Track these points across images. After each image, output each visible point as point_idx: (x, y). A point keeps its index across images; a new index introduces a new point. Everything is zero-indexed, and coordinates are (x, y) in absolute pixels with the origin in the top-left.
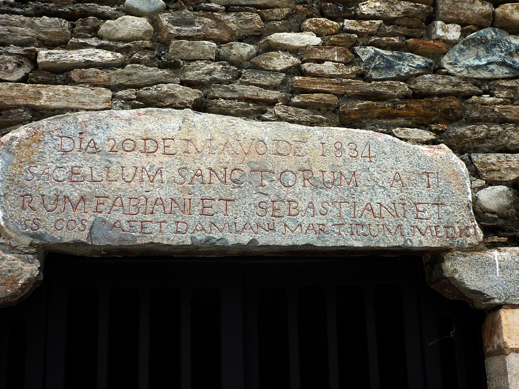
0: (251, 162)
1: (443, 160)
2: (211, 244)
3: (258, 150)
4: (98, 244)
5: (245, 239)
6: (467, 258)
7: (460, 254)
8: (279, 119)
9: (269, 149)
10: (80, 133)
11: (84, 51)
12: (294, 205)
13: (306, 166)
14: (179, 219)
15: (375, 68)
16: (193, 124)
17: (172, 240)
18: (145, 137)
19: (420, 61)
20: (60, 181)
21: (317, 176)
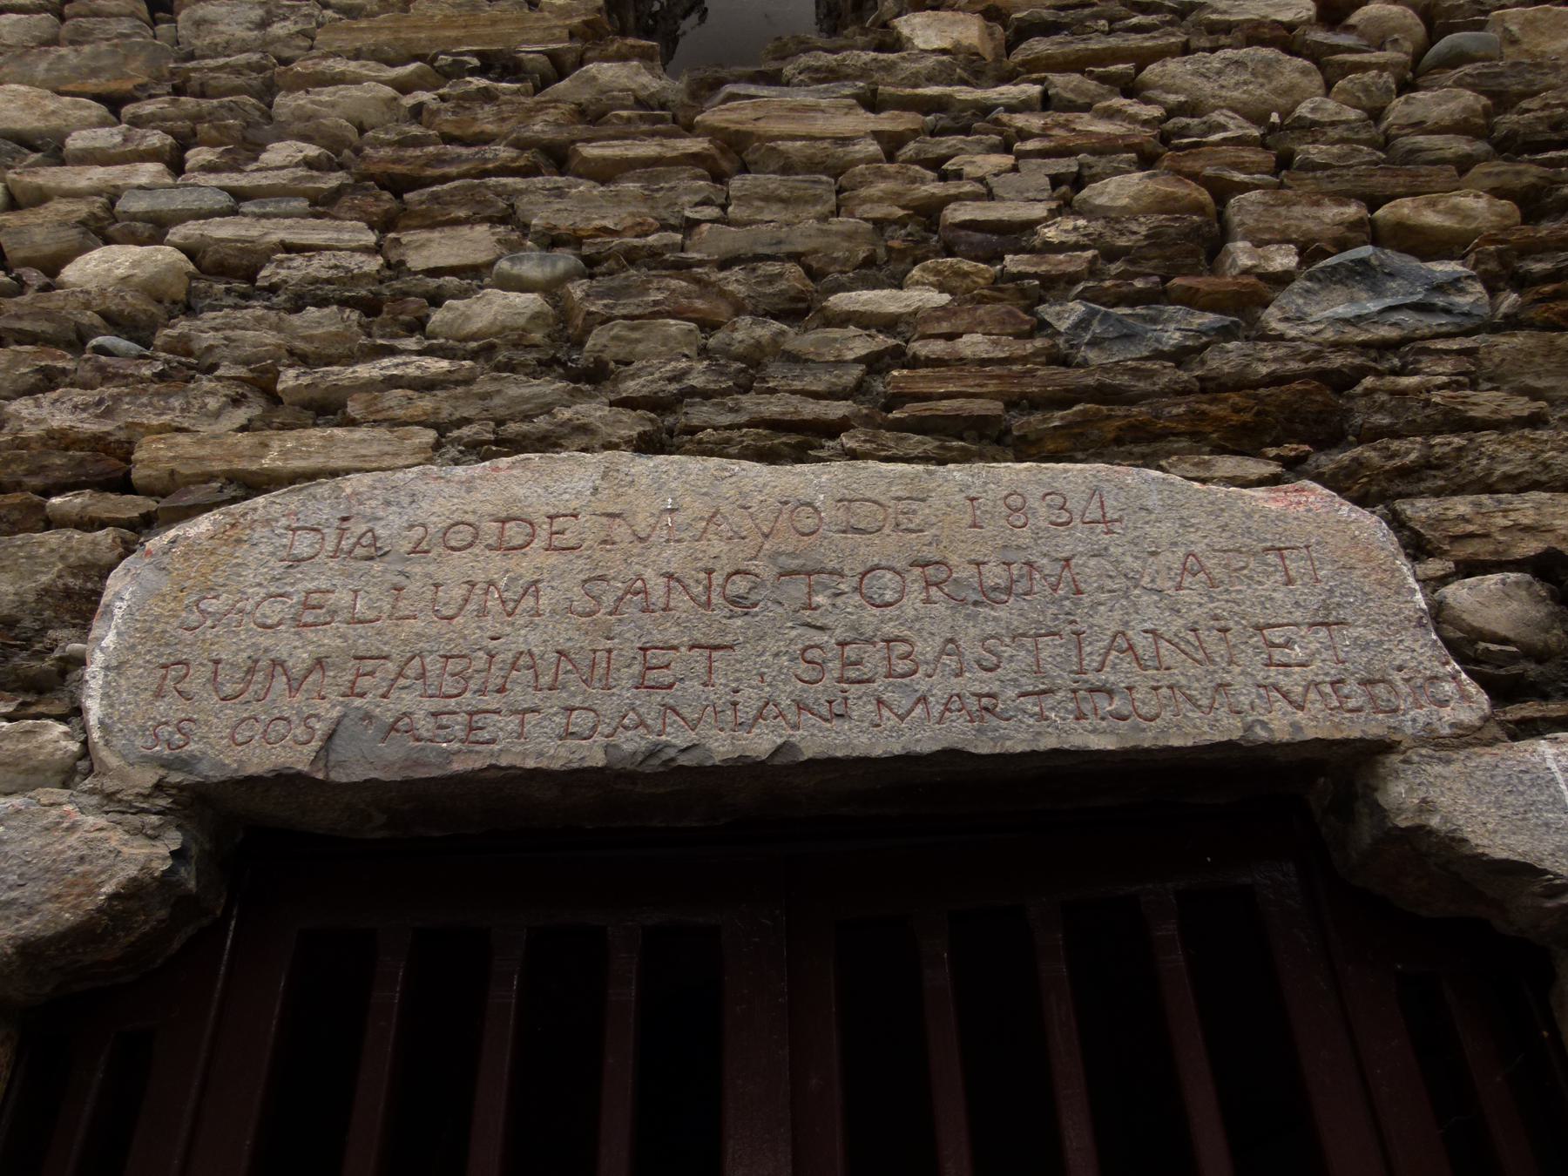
0: (781, 554)
1: (1318, 515)
2: (665, 763)
3: (798, 525)
4: (344, 780)
5: (761, 742)
6: (1452, 767)
7: (1431, 757)
8: (853, 455)
9: (827, 520)
10: (345, 519)
11: (386, 362)
12: (903, 648)
13: (931, 553)
14: (577, 702)
15: (1093, 343)
16: (629, 479)
17: (553, 757)
18: (504, 515)
20: (270, 627)
21: (965, 575)
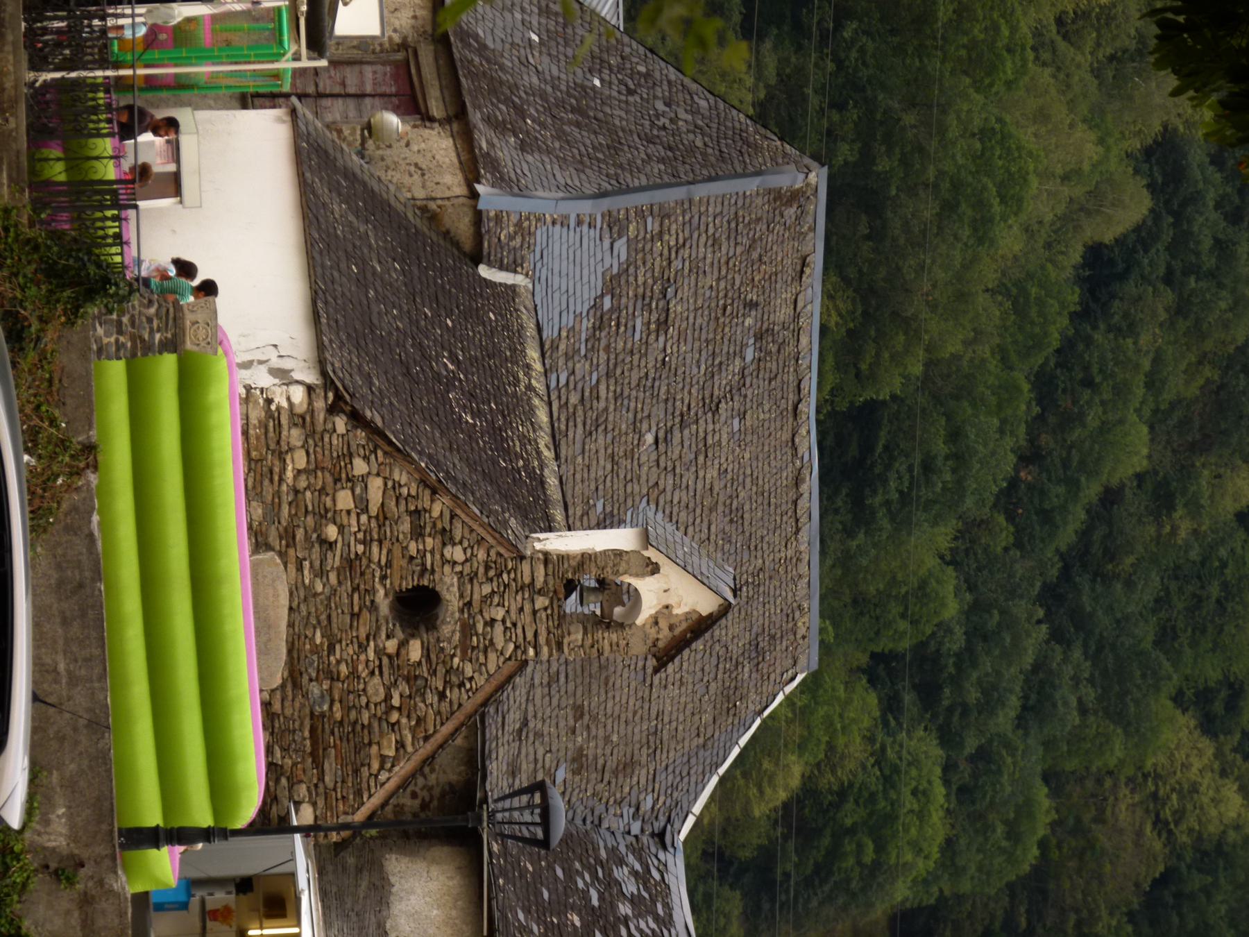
19: (314, 675)
